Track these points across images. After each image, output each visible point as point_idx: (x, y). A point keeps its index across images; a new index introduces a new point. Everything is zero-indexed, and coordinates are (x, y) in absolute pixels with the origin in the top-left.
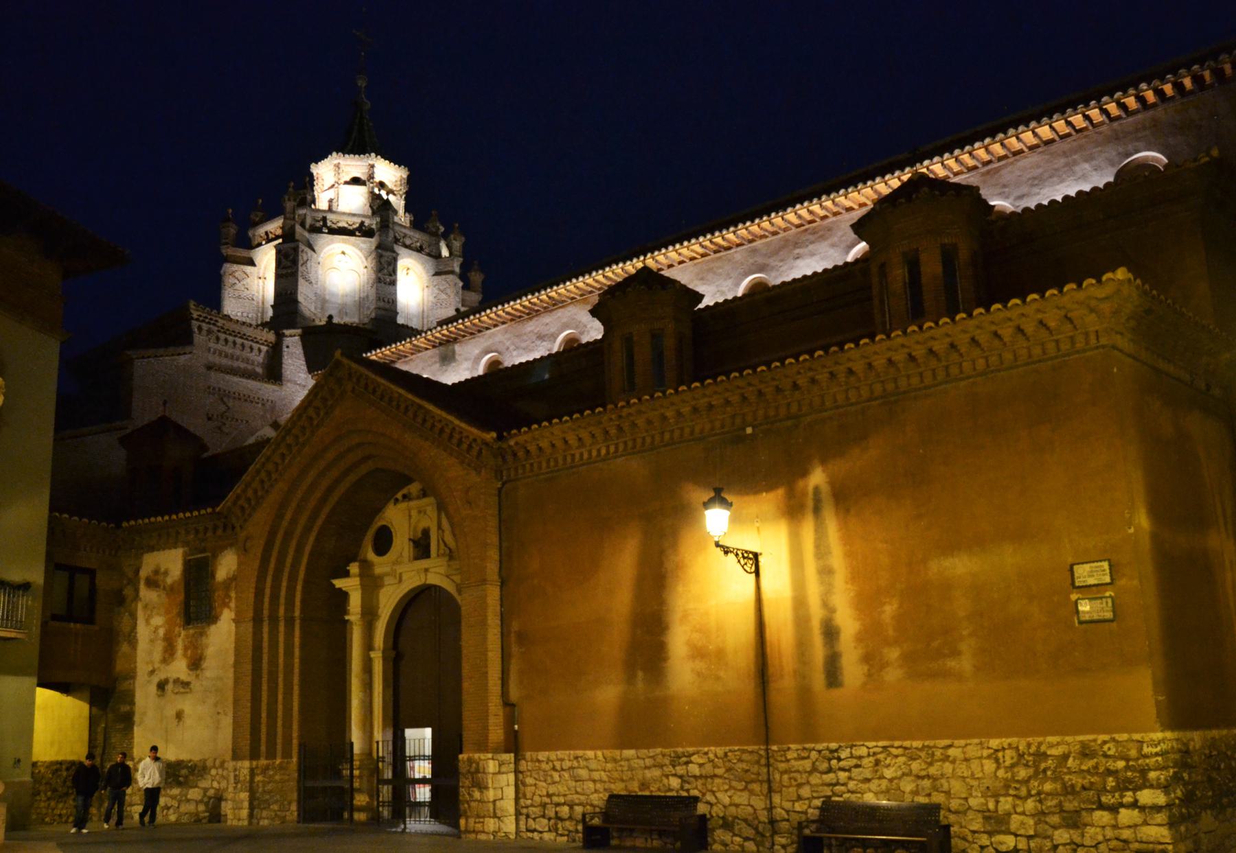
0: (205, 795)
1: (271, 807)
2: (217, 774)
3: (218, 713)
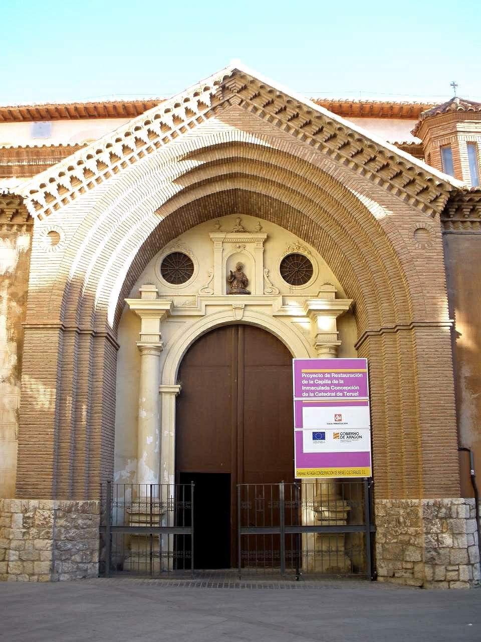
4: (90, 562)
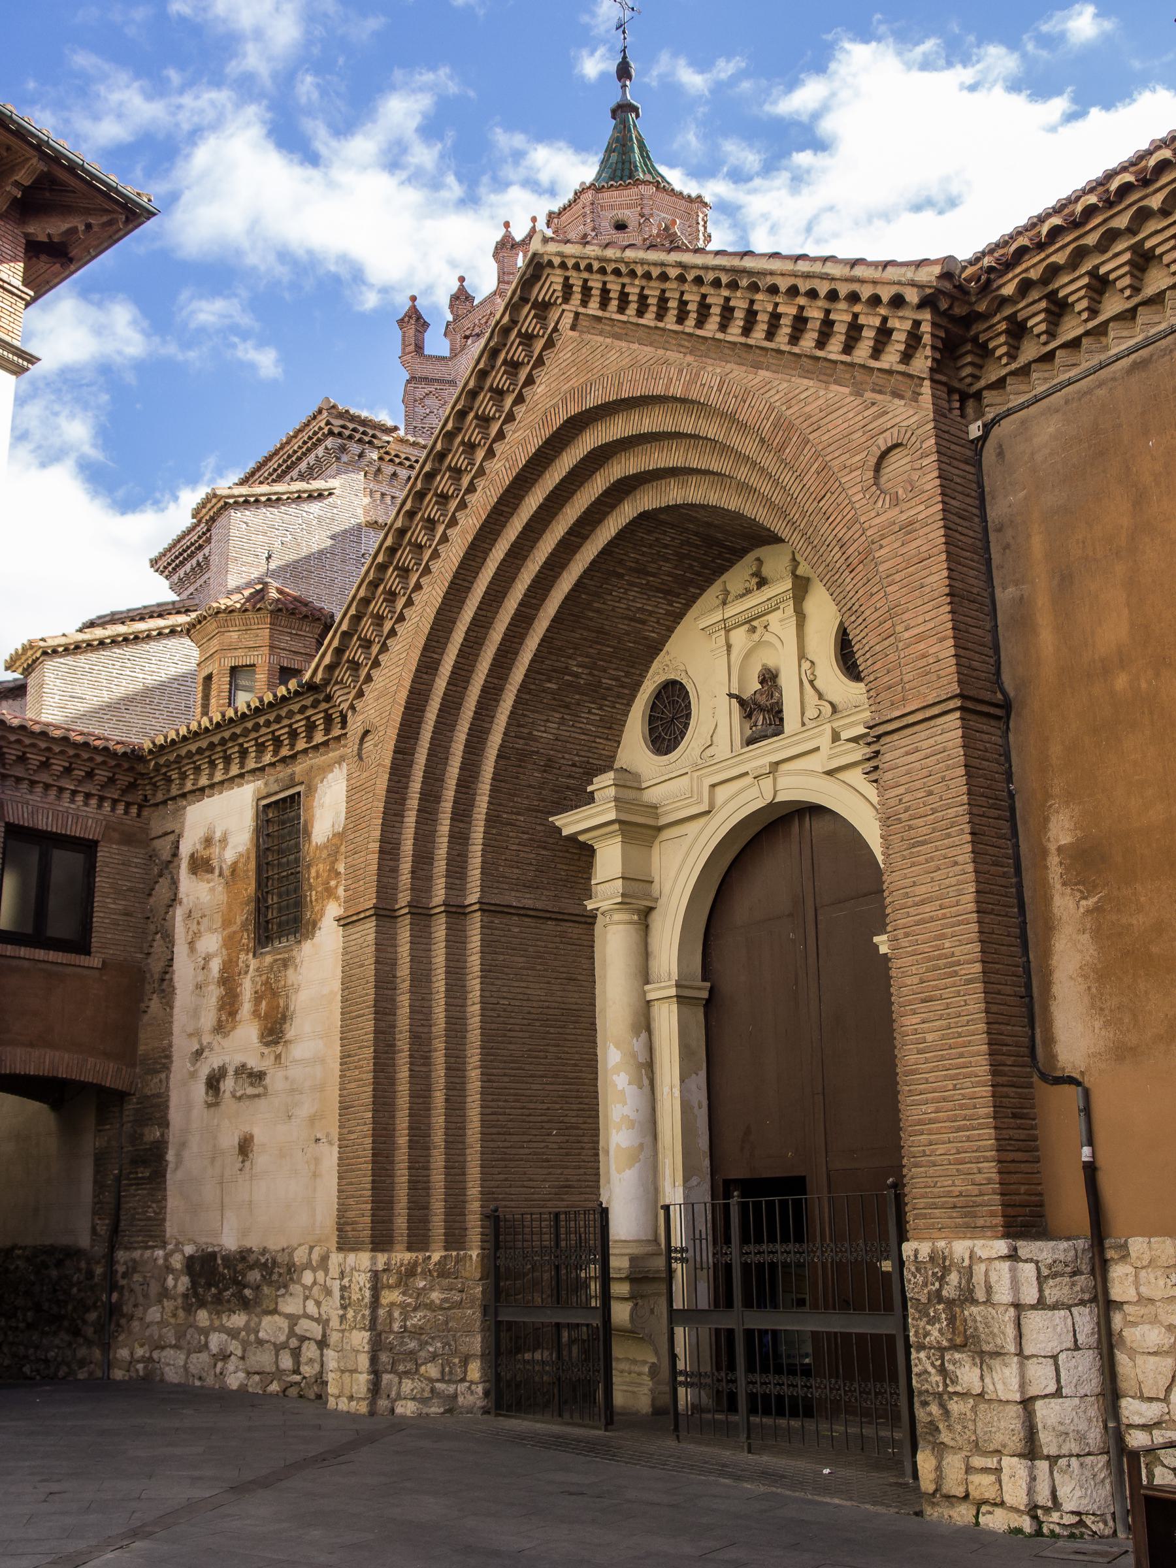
0: (292, 1333)
1: (423, 1369)
2: (315, 1283)
3: (317, 1140)
4: (463, 1380)
